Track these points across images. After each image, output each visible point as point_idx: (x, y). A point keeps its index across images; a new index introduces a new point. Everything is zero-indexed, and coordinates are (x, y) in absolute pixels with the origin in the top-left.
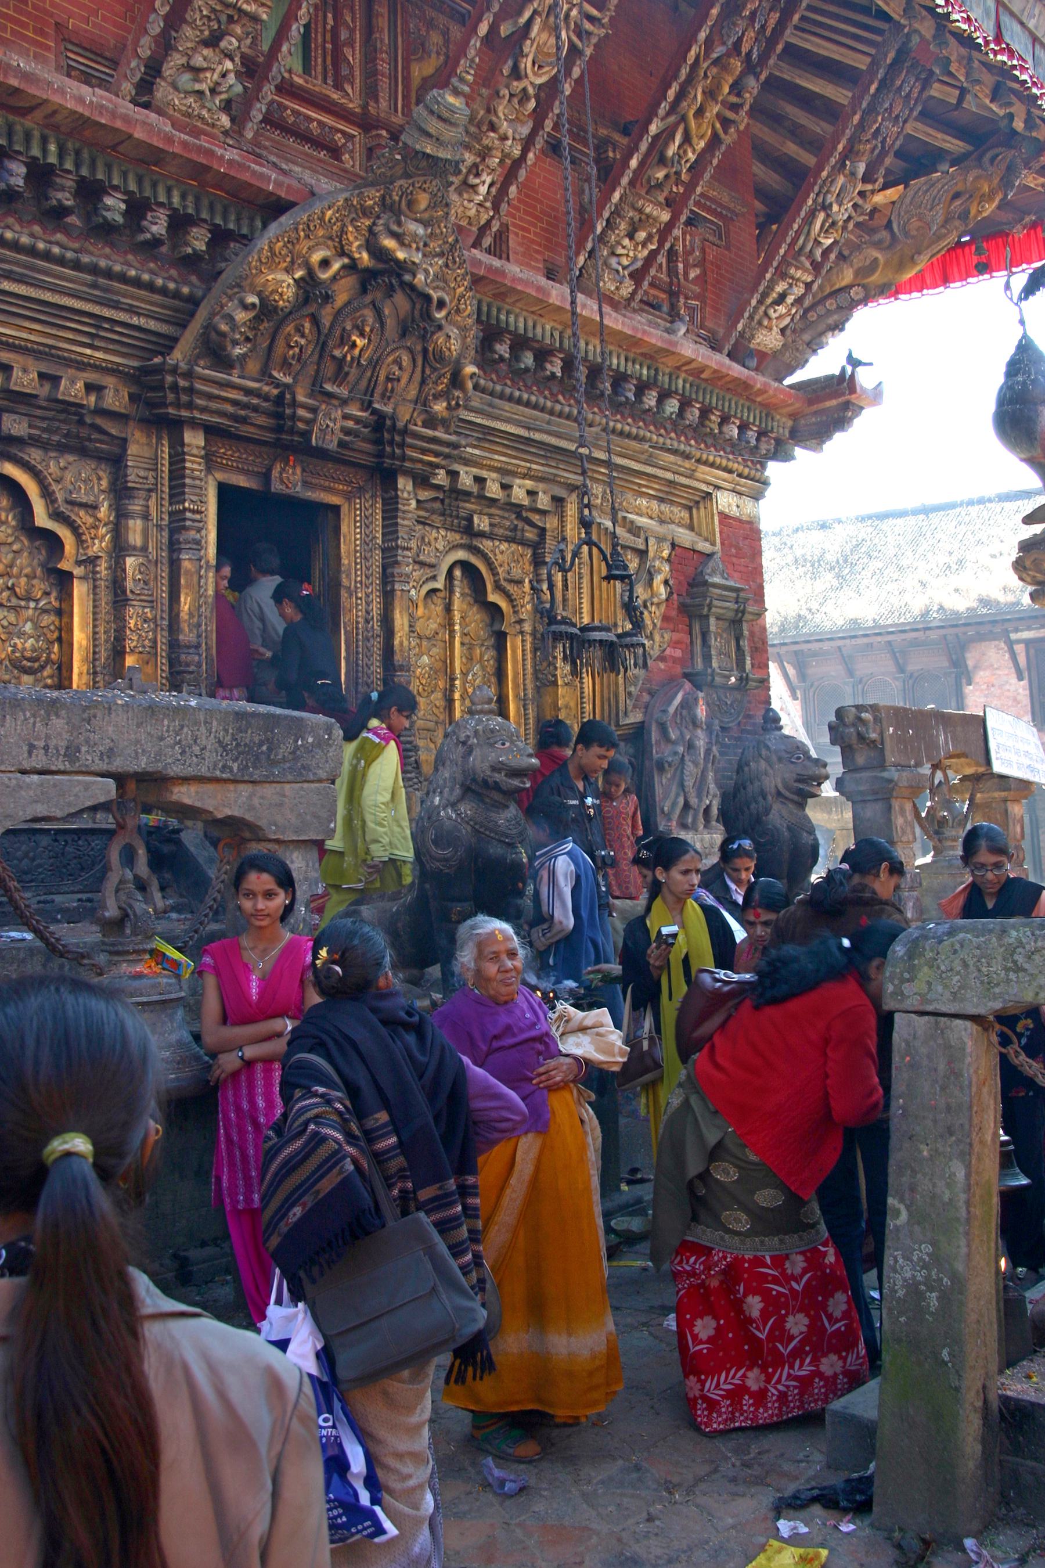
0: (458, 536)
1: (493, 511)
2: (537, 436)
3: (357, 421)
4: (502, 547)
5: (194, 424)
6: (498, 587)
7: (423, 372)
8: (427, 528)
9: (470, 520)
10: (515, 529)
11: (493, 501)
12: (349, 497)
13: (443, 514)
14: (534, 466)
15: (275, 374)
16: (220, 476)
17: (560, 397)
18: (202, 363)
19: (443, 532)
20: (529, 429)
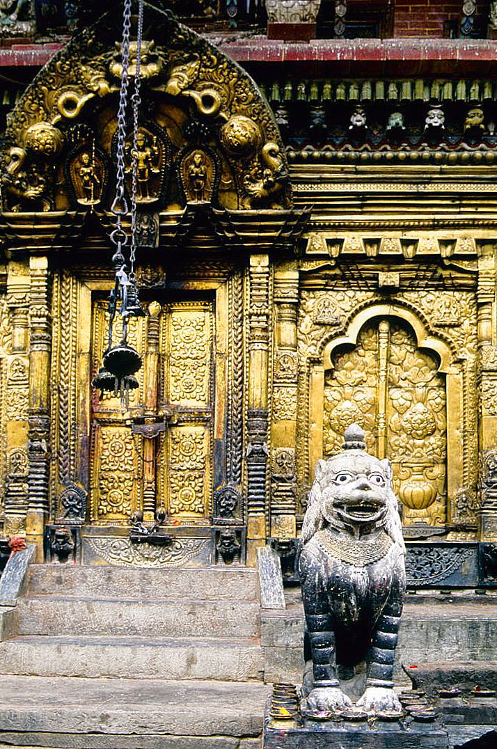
0: (371, 294)
1: (406, 266)
2: (431, 188)
3: (177, 218)
4: (430, 297)
5: (39, 254)
6: (431, 333)
7: (229, 163)
8: (330, 293)
9: (376, 278)
10: (441, 278)
11: (399, 259)
12: (226, 278)
13: (343, 278)
14: (438, 217)
15: (82, 201)
16: (95, 286)
17: (465, 145)
18: (14, 208)
19: (351, 293)
20: (417, 183)
